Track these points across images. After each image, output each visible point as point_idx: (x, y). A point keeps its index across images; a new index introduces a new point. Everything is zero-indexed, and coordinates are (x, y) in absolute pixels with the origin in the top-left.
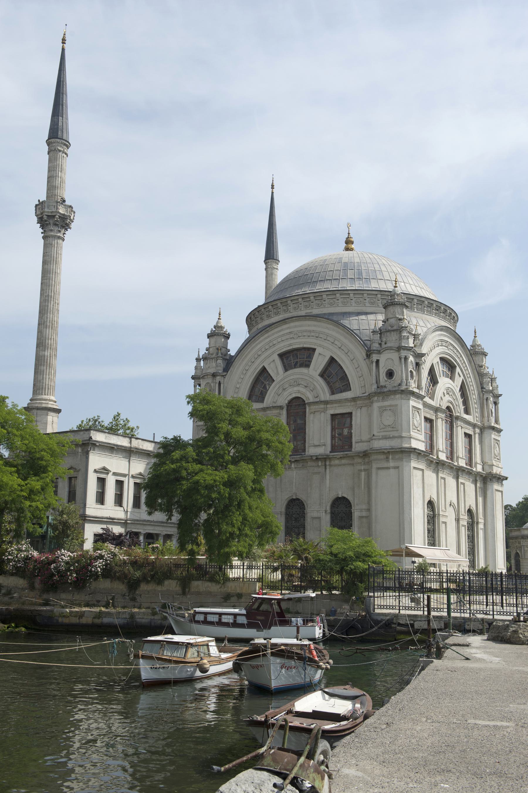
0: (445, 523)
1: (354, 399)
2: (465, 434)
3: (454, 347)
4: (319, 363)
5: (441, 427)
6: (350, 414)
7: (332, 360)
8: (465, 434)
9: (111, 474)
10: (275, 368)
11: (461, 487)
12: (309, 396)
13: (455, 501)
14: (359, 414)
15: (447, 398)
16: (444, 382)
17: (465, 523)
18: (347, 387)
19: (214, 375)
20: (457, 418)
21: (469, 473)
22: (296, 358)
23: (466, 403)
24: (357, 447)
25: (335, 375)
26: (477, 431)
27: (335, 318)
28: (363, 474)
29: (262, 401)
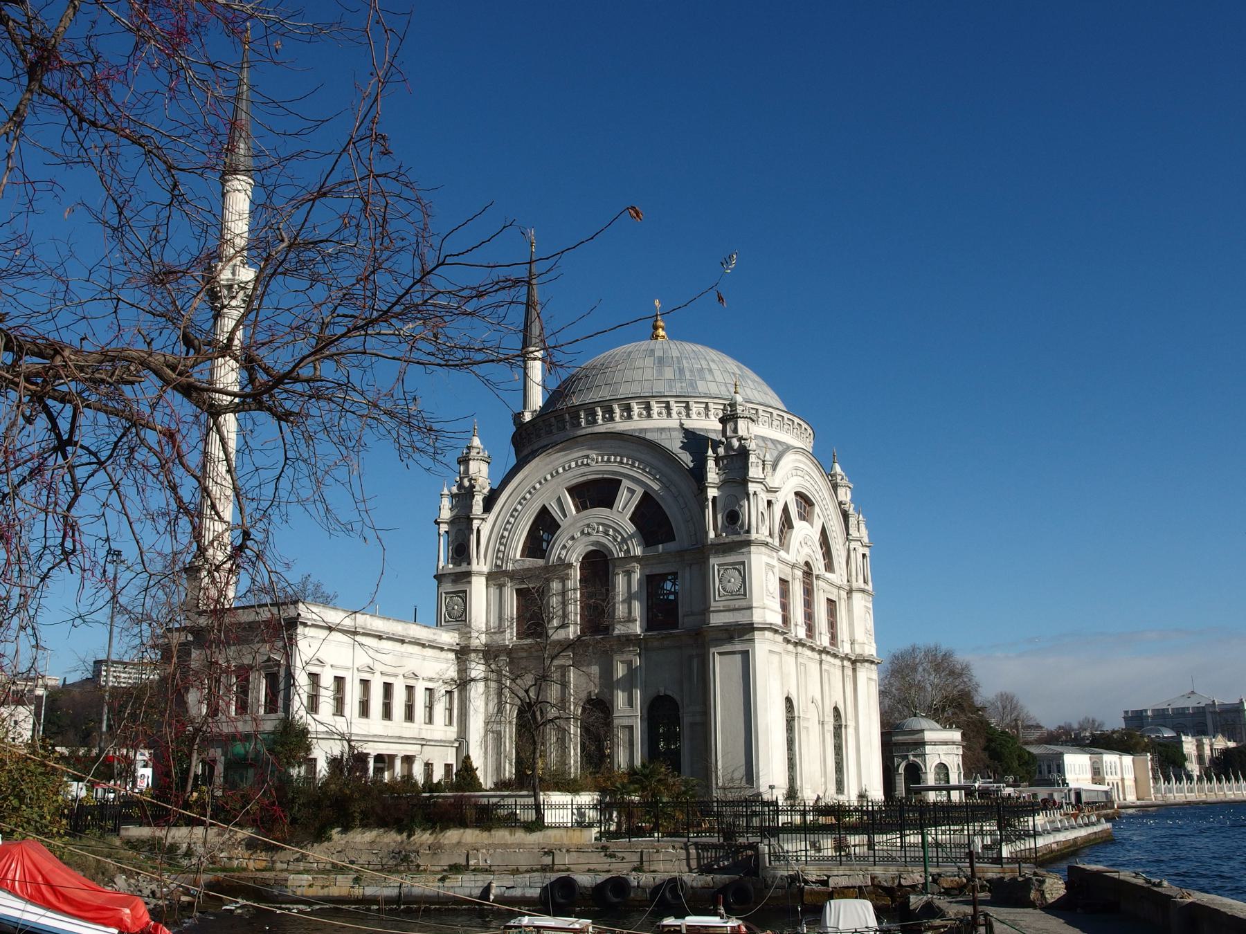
0: (807, 728)
1: (681, 553)
2: (828, 599)
3: (812, 477)
5: (797, 590)
6: (675, 574)
8: (828, 599)
9: (328, 667)
11: (825, 675)
13: (818, 697)
14: (687, 575)
15: (806, 550)
16: (801, 529)
17: (832, 728)
18: (670, 537)
20: (818, 577)
21: (835, 656)
23: (828, 554)
24: (686, 621)
26: (844, 594)
28: (695, 660)
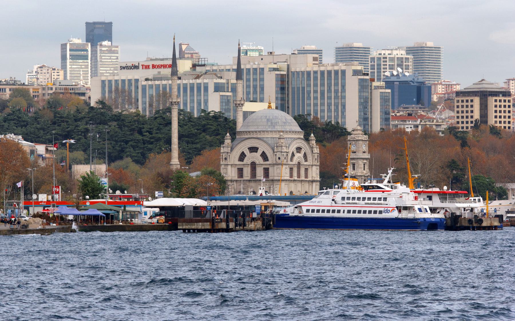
1: (270, 164)
4: (260, 152)
7: (263, 152)
10: (247, 152)
12: (257, 162)
18: (268, 160)
19: (228, 153)
22: (254, 150)
25: (264, 156)
27: (265, 139)
29: (243, 161)
